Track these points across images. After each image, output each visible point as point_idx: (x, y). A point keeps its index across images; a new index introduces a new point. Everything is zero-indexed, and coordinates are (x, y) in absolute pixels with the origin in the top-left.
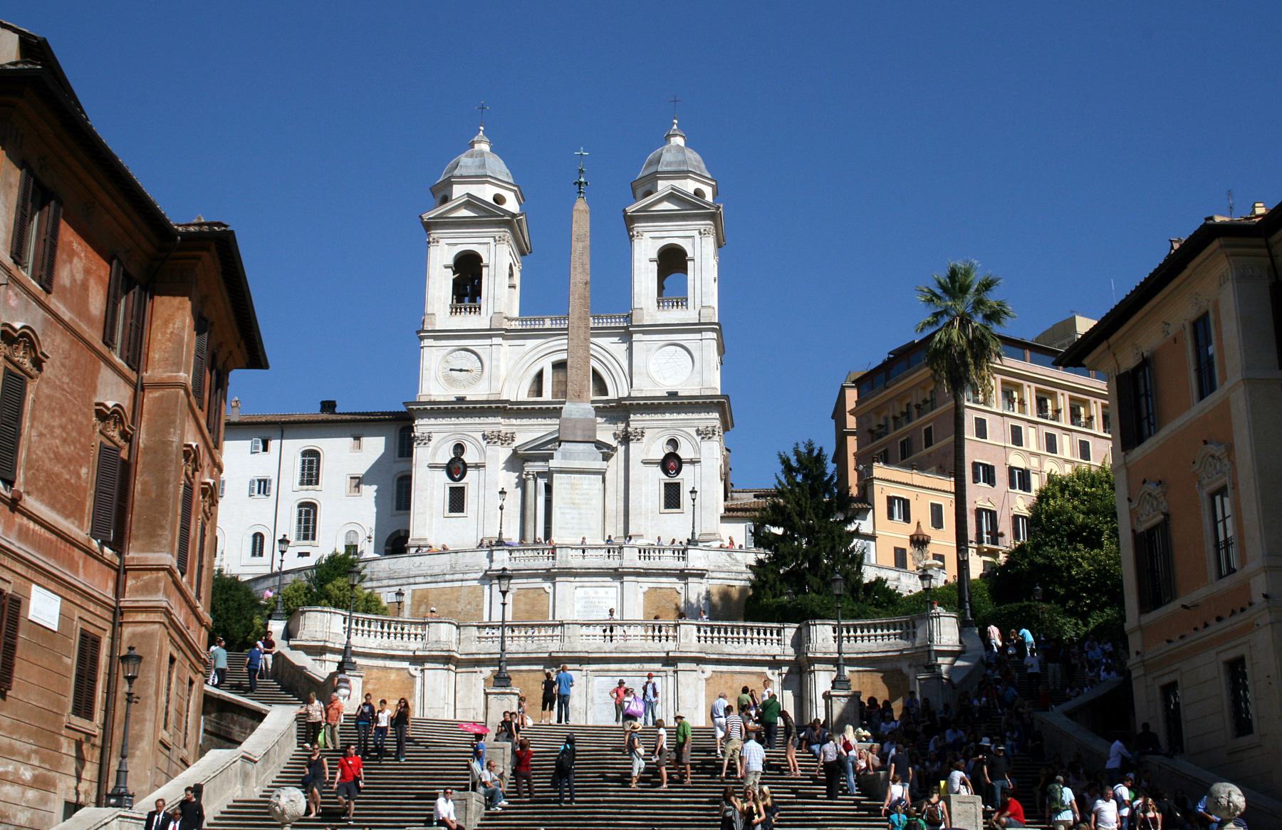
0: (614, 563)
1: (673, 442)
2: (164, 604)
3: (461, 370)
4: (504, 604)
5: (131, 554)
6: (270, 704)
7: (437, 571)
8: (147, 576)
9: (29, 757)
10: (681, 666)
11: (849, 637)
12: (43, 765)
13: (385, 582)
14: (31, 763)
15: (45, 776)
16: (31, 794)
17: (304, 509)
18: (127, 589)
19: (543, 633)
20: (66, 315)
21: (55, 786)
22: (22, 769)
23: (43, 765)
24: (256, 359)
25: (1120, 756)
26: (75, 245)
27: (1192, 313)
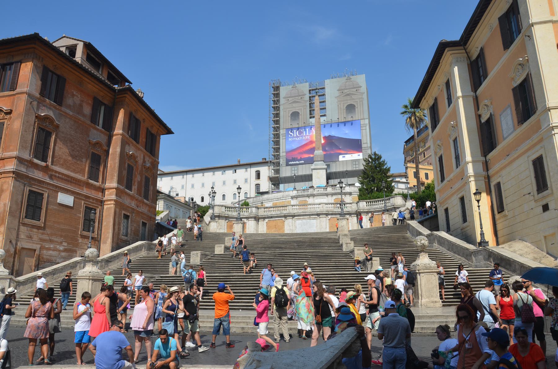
0: (326, 192)
2: (115, 198)
4: (239, 197)
5: (107, 184)
7: (279, 197)
8: (111, 191)
9: (61, 243)
10: (321, 216)
11: (371, 205)
13: (266, 201)
15: (71, 249)
16: (63, 254)
17: (257, 186)
18: (106, 195)
19: (284, 209)
20: (71, 113)
21: (77, 252)
22: (58, 246)
24: (169, 131)
26: (75, 93)
27: (445, 80)
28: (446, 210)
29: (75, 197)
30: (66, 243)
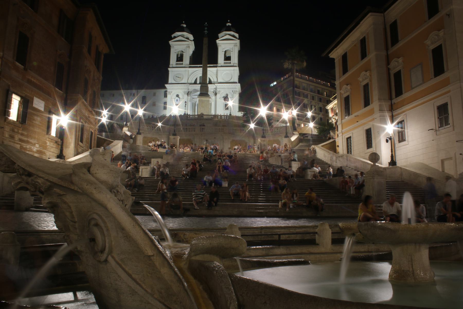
1: (227, 95)
3: (178, 77)
6: (114, 140)
12: (40, 147)
14: (36, 146)
22: (32, 148)
23: (40, 147)
25: (337, 153)
28: (349, 139)
29: (45, 103)
30: (38, 145)
